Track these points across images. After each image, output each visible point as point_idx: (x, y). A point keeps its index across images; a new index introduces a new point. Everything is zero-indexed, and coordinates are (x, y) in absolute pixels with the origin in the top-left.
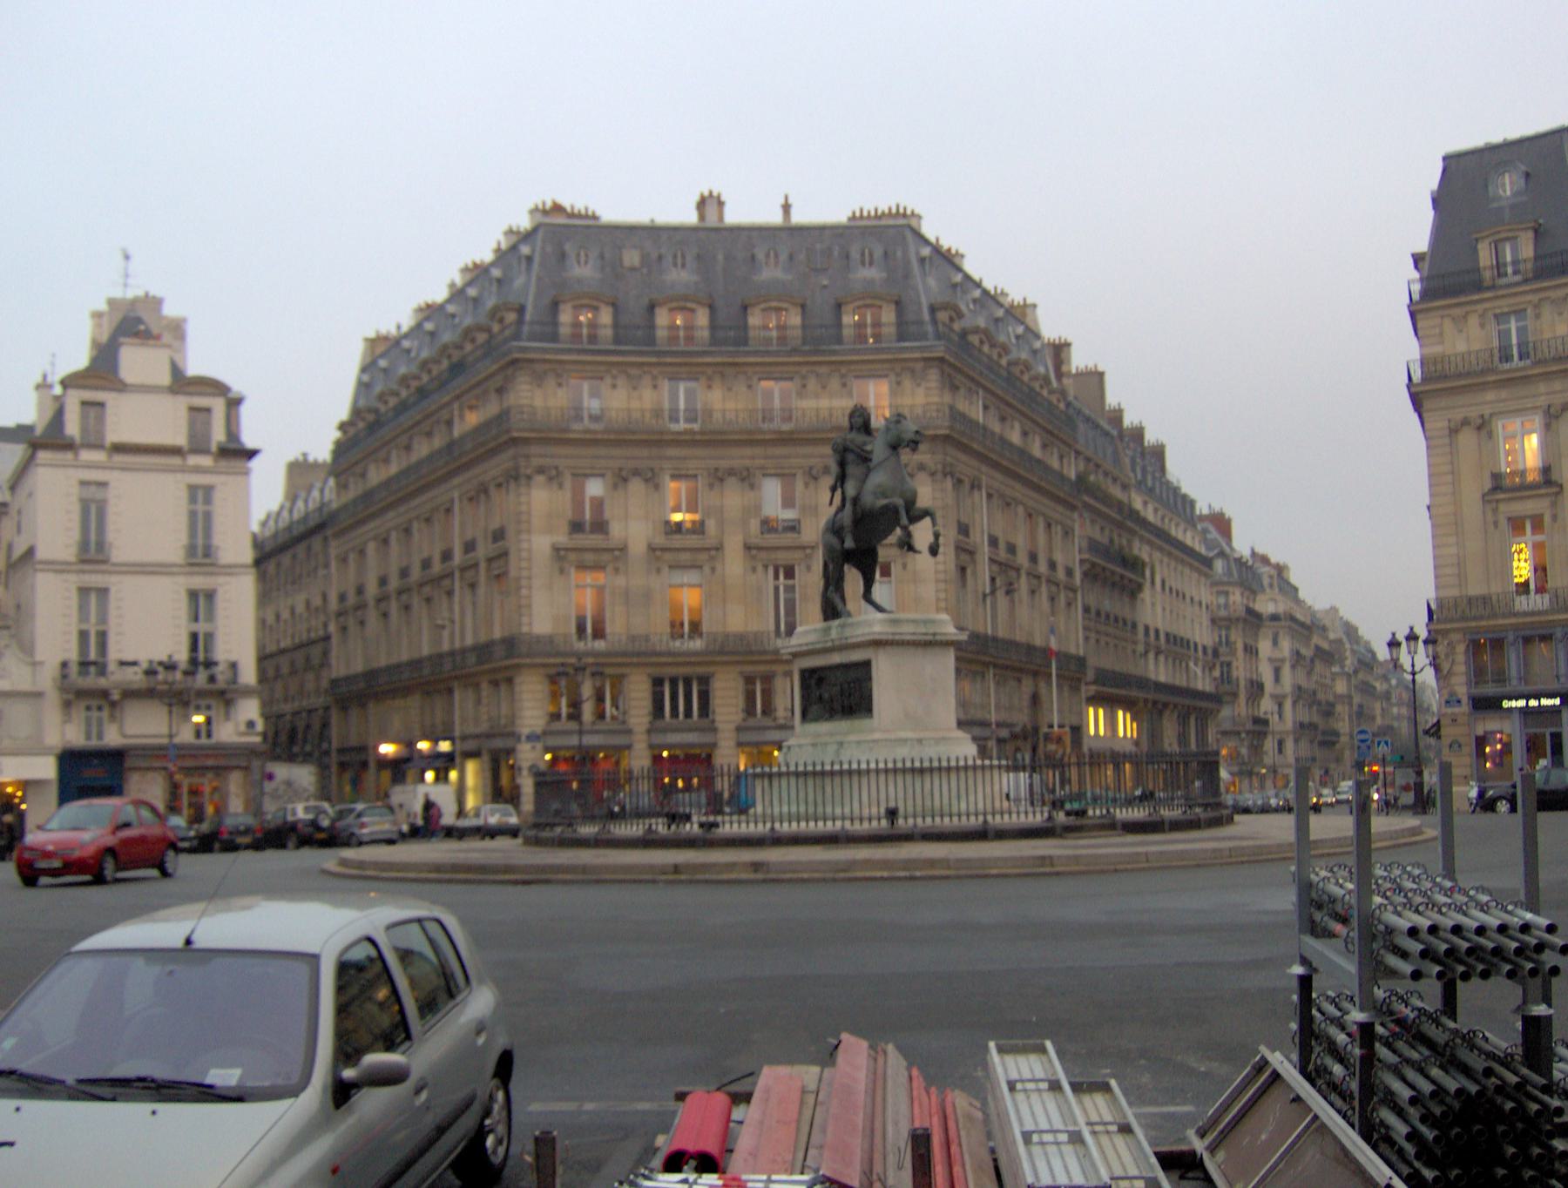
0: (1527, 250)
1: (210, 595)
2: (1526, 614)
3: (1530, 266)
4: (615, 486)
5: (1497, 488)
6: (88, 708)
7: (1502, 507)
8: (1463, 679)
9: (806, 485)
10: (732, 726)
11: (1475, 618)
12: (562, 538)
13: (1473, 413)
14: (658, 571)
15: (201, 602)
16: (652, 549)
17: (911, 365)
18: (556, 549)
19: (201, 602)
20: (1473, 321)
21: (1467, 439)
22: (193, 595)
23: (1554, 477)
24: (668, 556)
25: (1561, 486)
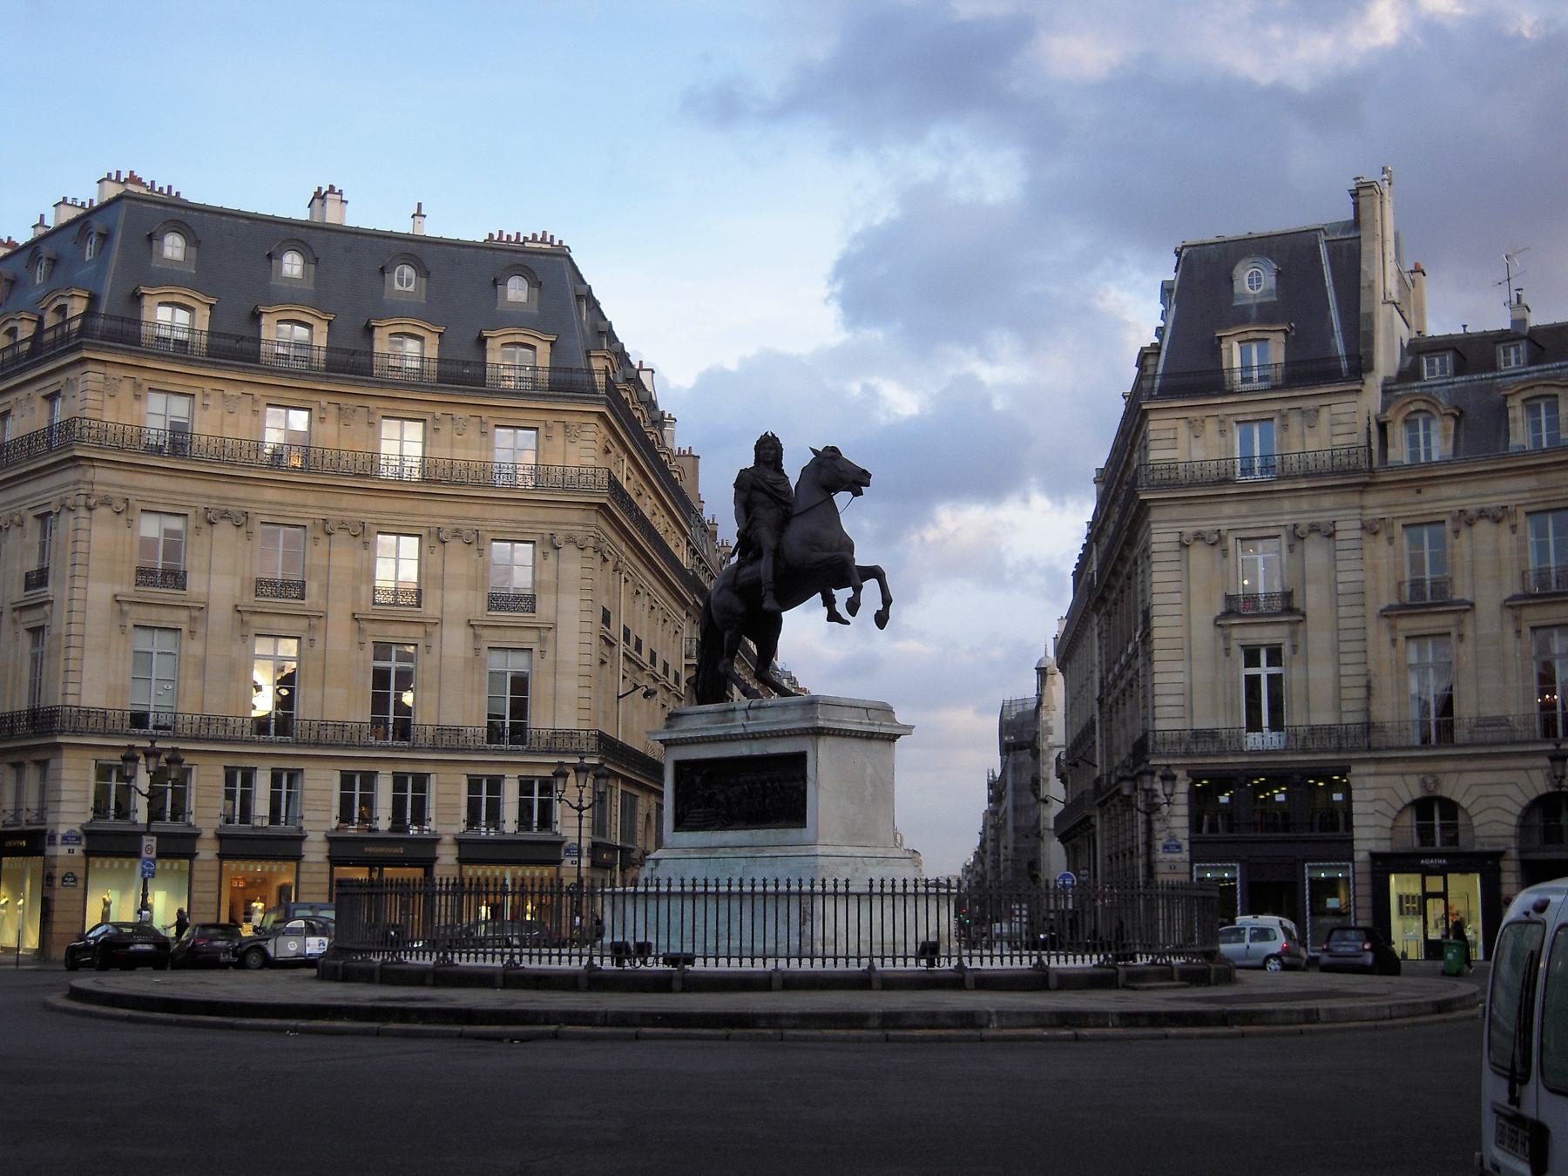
0: (1277, 353)
2: (1259, 753)
3: (1280, 372)
5: (1228, 613)
7: (1235, 633)
8: (1185, 822)
10: (321, 836)
11: (1202, 755)
12: (127, 588)
13: (1206, 527)
14: (244, 636)
17: (565, 418)
20: (1211, 427)
21: (1200, 556)
23: (1297, 604)
24: (257, 621)
25: (1304, 615)
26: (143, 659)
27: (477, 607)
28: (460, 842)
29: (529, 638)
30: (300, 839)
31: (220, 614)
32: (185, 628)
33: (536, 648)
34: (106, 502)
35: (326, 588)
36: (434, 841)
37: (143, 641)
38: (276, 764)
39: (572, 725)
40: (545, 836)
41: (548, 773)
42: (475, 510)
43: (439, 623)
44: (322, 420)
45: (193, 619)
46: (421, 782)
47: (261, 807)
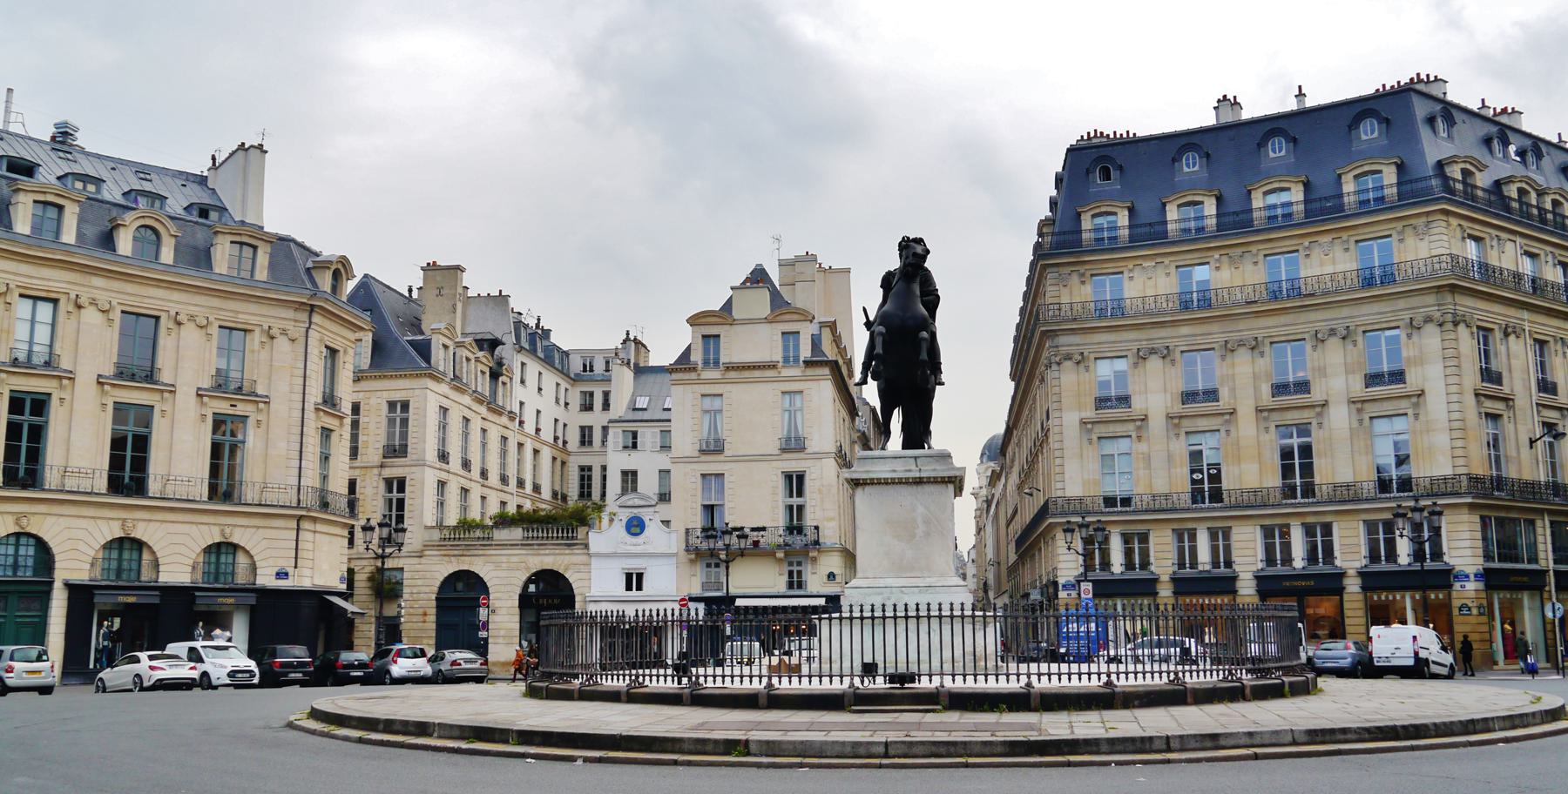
1: (801, 478)
4: (1136, 365)
6: (709, 565)
9: (1315, 348)
10: (1250, 576)
12: (1090, 413)
14: (1177, 435)
15: (796, 483)
16: (1169, 417)
18: (1083, 423)
19: (796, 483)
22: (788, 477)
24: (1185, 422)
26: (1107, 459)
27: (1357, 387)
28: (1362, 574)
29: (1404, 405)
30: (1234, 579)
31: (1157, 423)
32: (1134, 435)
33: (1410, 412)
34: (1068, 357)
35: (1233, 390)
36: (1342, 575)
37: (1110, 448)
38: (1210, 524)
39: (1448, 471)
40: (1327, 569)
41: (1388, 516)
42: (1345, 312)
43: (1325, 404)
44: (1218, 268)
45: (1139, 428)
46: (1327, 530)
47: (1204, 555)
